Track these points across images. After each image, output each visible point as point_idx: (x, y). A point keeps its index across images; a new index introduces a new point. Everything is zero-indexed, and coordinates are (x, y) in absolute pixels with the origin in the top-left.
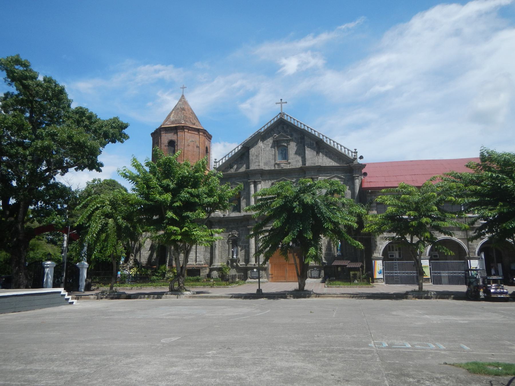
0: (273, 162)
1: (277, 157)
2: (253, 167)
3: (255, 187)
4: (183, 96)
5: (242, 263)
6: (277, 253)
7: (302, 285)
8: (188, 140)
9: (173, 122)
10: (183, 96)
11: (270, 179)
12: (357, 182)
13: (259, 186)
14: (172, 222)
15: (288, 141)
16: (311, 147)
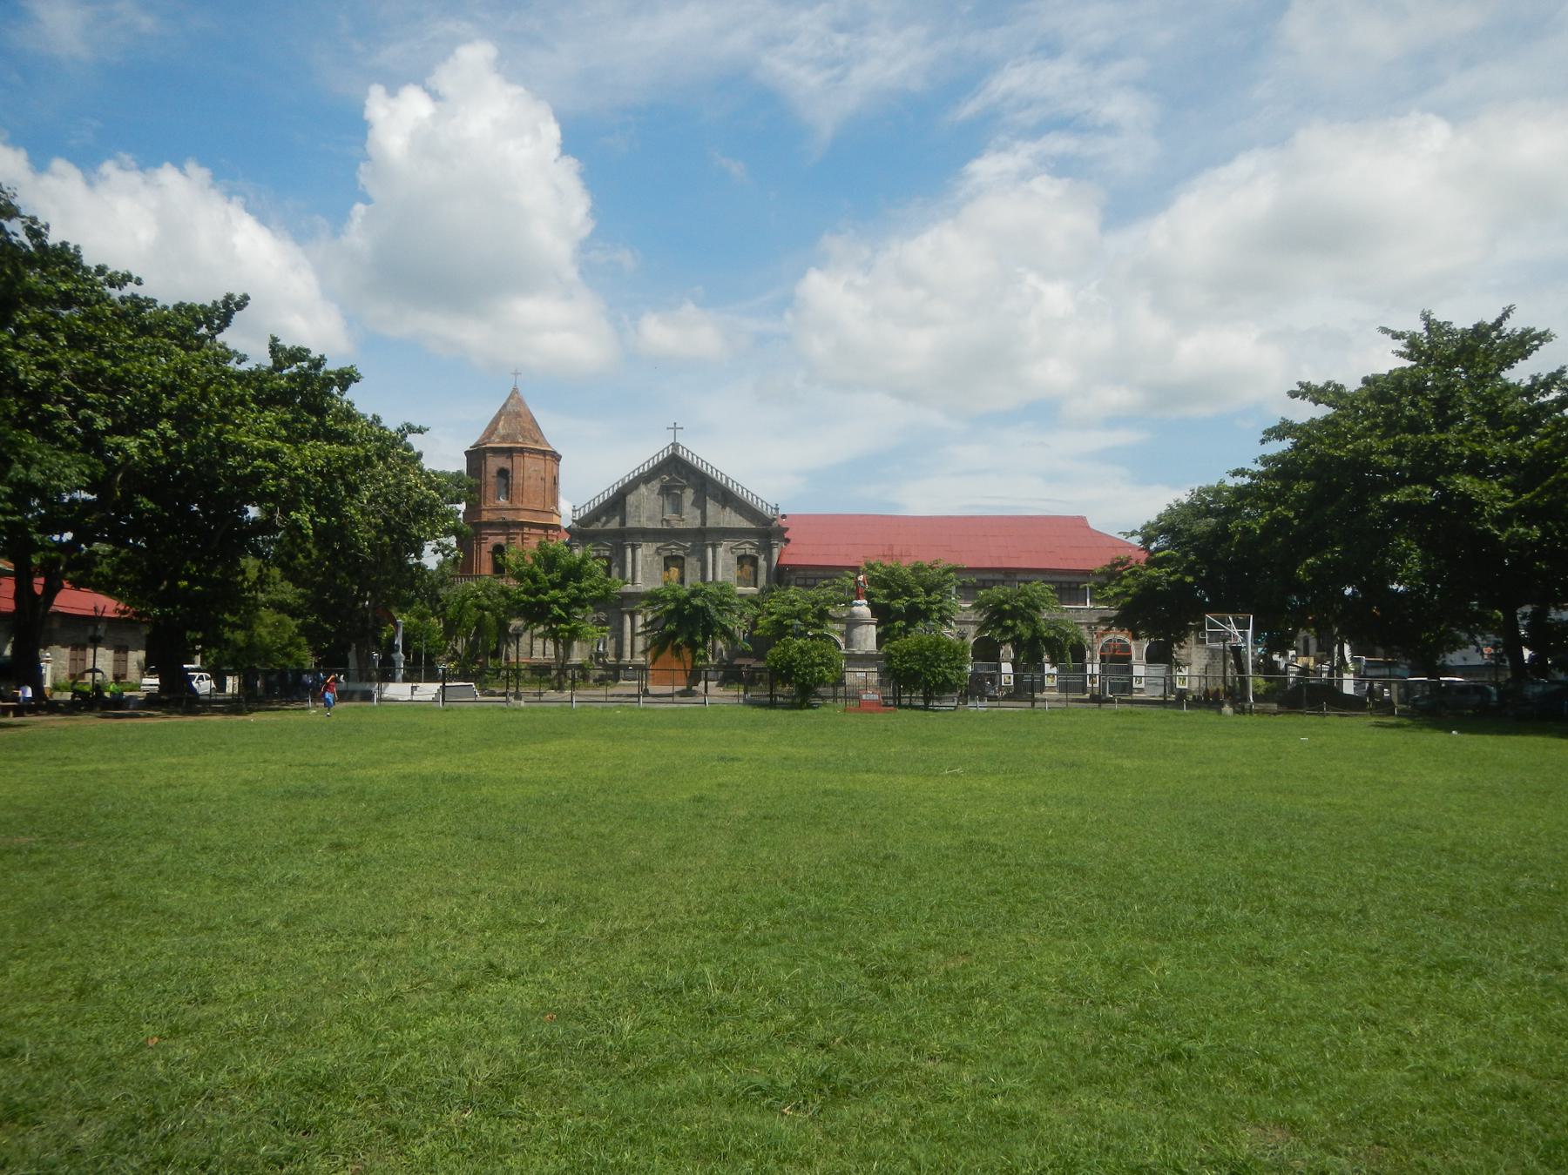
0: (659, 517)
1: (668, 509)
2: (631, 524)
3: (633, 552)
4: (515, 390)
5: (611, 659)
6: (667, 654)
7: (689, 689)
8: (528, 468)
9: (504, 438)
10: (515, 390)
11: (655, 541)
12: (776, 551)
13: (639, 551)
14: (559, 619)
15: (683, 488)
16: (714, 498)
